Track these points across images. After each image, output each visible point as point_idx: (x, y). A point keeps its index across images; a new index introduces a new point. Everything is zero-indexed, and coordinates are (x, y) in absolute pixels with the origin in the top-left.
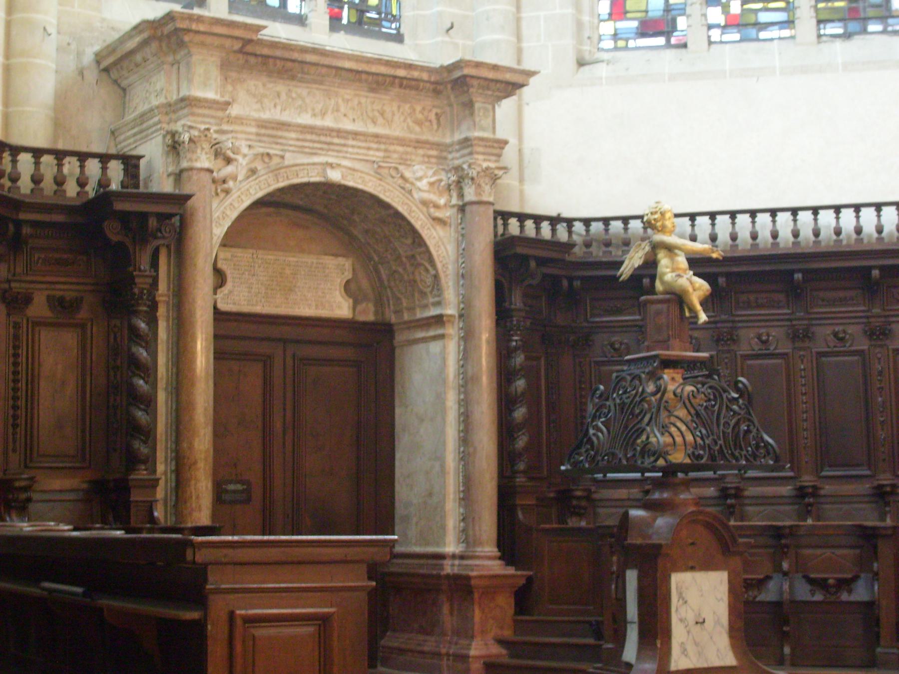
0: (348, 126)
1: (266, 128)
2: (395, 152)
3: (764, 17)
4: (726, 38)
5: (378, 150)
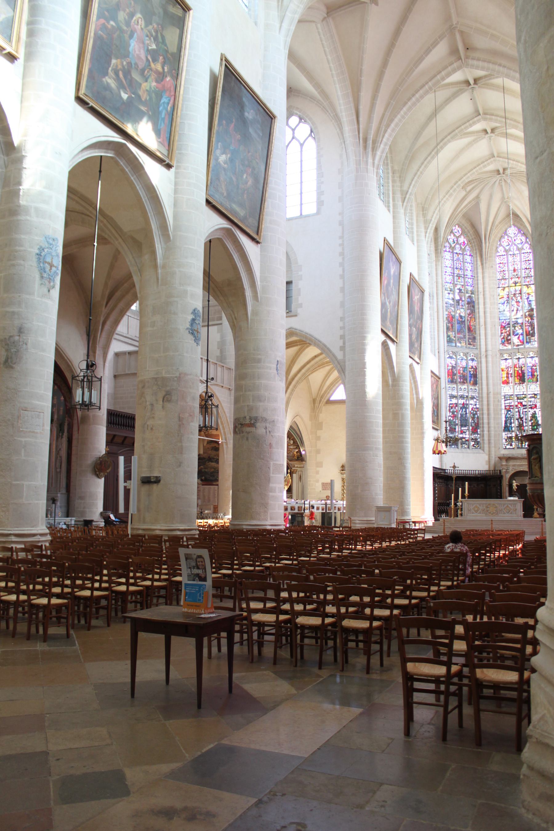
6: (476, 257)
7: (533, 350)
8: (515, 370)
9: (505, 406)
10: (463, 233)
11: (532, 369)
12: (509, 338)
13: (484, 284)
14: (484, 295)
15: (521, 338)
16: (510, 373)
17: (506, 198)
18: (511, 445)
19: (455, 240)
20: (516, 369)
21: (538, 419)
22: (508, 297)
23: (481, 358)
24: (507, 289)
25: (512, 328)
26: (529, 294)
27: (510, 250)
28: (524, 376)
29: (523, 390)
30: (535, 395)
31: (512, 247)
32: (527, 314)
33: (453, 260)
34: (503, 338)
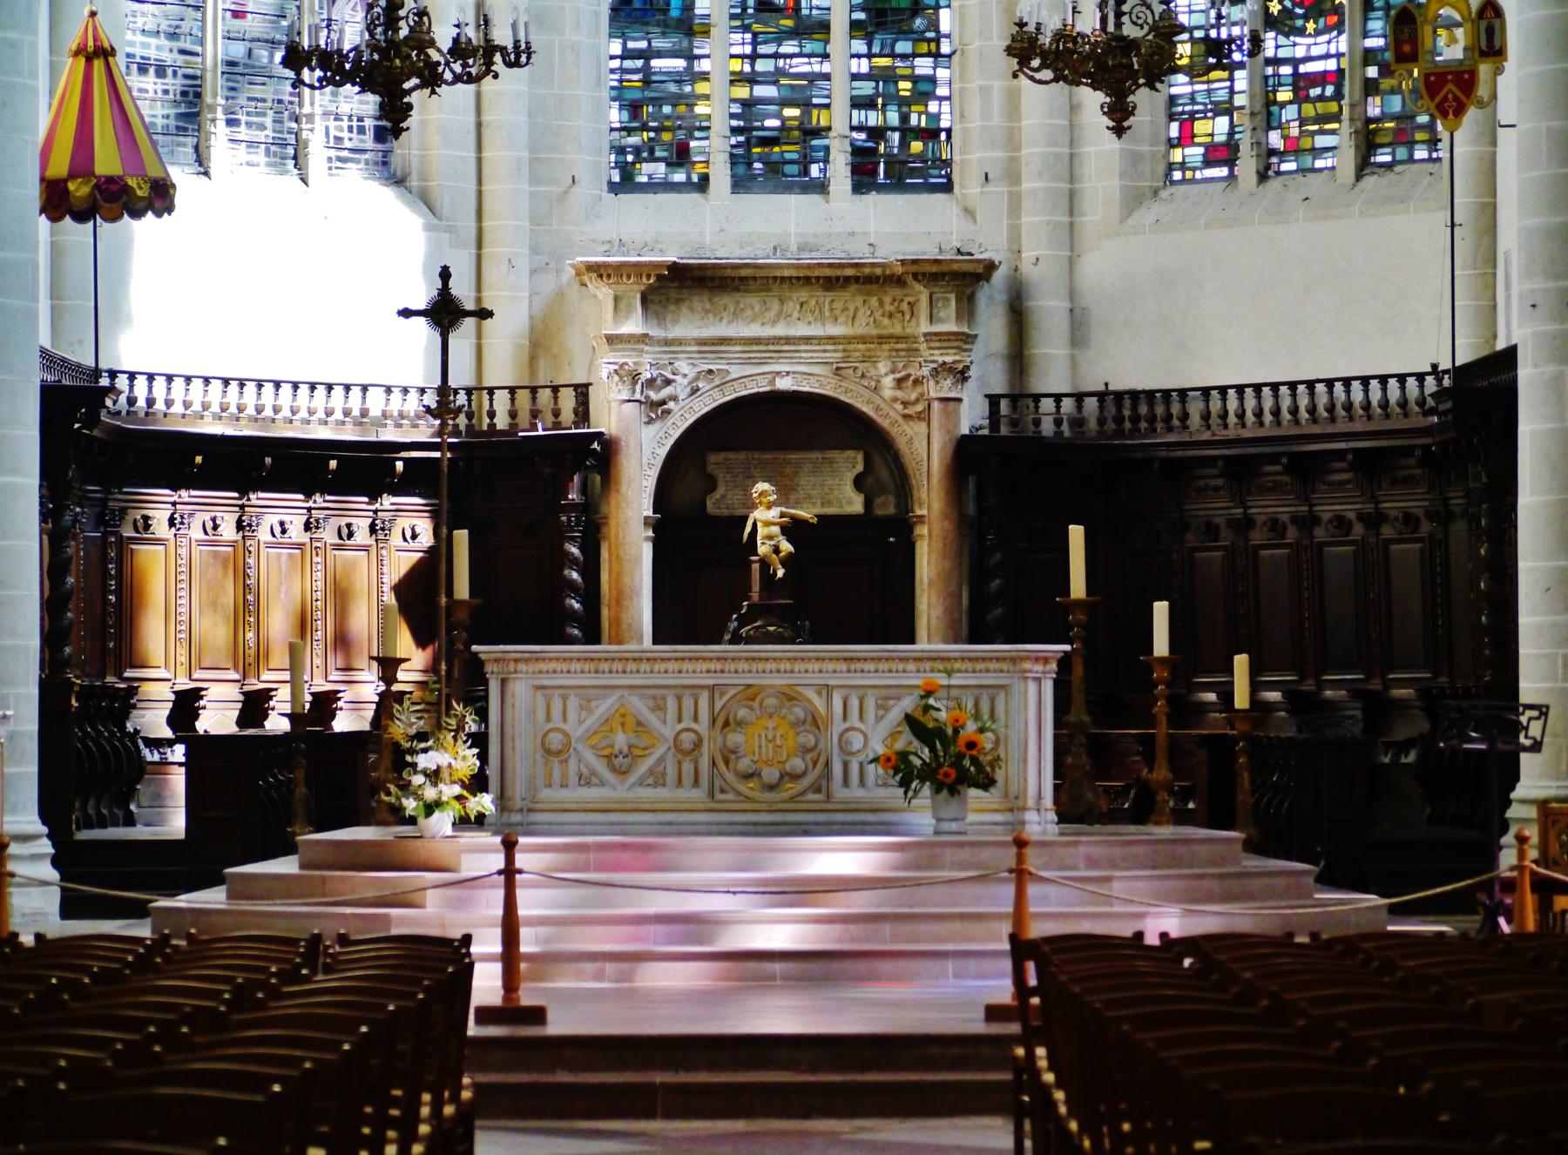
0: (801, 330)
1: (705, 344)
2: (855, 350)
3: (1321, 141)
4: (1285, 167)
5: (835, 351)
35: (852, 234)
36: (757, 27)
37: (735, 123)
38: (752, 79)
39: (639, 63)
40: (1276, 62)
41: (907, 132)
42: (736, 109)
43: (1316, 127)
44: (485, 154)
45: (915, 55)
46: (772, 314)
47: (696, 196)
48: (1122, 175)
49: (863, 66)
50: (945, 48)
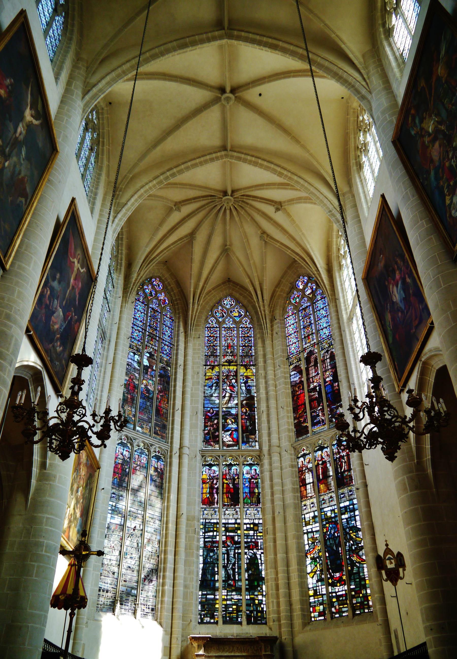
3: (344, 609)
6: (179, 322)
7: (252, 453)
8: (223, 483)
9: (205, 542)
10: (165, 289)
11: (250, 482)
12: (217, 434)
13: (185, 356)
14: (184, 370)
15: (235, 436)
16: (216, 486)
17: (228, 244)
18: (212, 617)
19: (153, 293)
20: (226, 482)
21: (260, 568)
22: (218, 379)
23: (171, 457)
24: (217, 369)
25: (221, 421)
26: (247, 377)
27: (224, 322)
28: (238, 494)
29: (236, 516)
30: (255, 524)
31: (227, 320)
32: (245, 402)
33: (147, 314)
34: (208, 434)
35: (247, 633)
36: (228, 589)
37: (223, 609)
38: (227, 600)
39: (205, 596)
40: (332, 593)
41: (258, 612)
42: (223, 606)
43: (342, 606)
44: (174, 614)
45: (258, 595)
46: (231, 650)
47: (215, 625)
48: (302, 619)
49: (248, 597)
50: (264, 594)
